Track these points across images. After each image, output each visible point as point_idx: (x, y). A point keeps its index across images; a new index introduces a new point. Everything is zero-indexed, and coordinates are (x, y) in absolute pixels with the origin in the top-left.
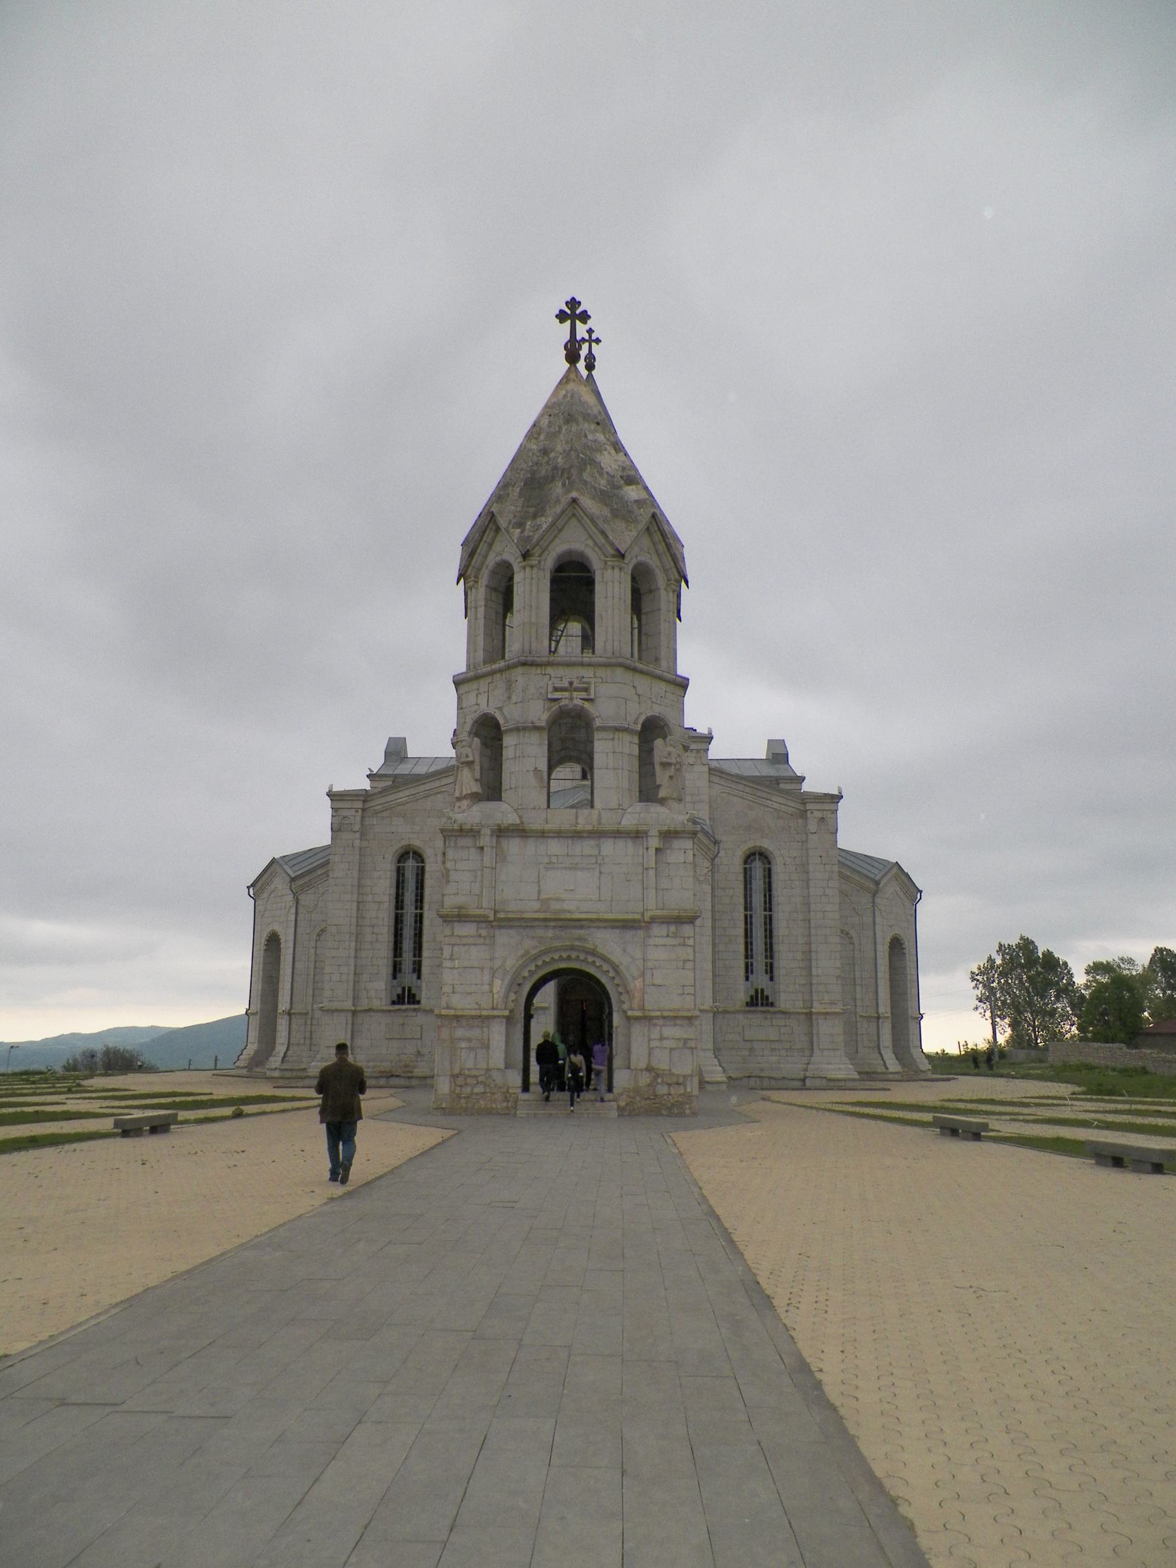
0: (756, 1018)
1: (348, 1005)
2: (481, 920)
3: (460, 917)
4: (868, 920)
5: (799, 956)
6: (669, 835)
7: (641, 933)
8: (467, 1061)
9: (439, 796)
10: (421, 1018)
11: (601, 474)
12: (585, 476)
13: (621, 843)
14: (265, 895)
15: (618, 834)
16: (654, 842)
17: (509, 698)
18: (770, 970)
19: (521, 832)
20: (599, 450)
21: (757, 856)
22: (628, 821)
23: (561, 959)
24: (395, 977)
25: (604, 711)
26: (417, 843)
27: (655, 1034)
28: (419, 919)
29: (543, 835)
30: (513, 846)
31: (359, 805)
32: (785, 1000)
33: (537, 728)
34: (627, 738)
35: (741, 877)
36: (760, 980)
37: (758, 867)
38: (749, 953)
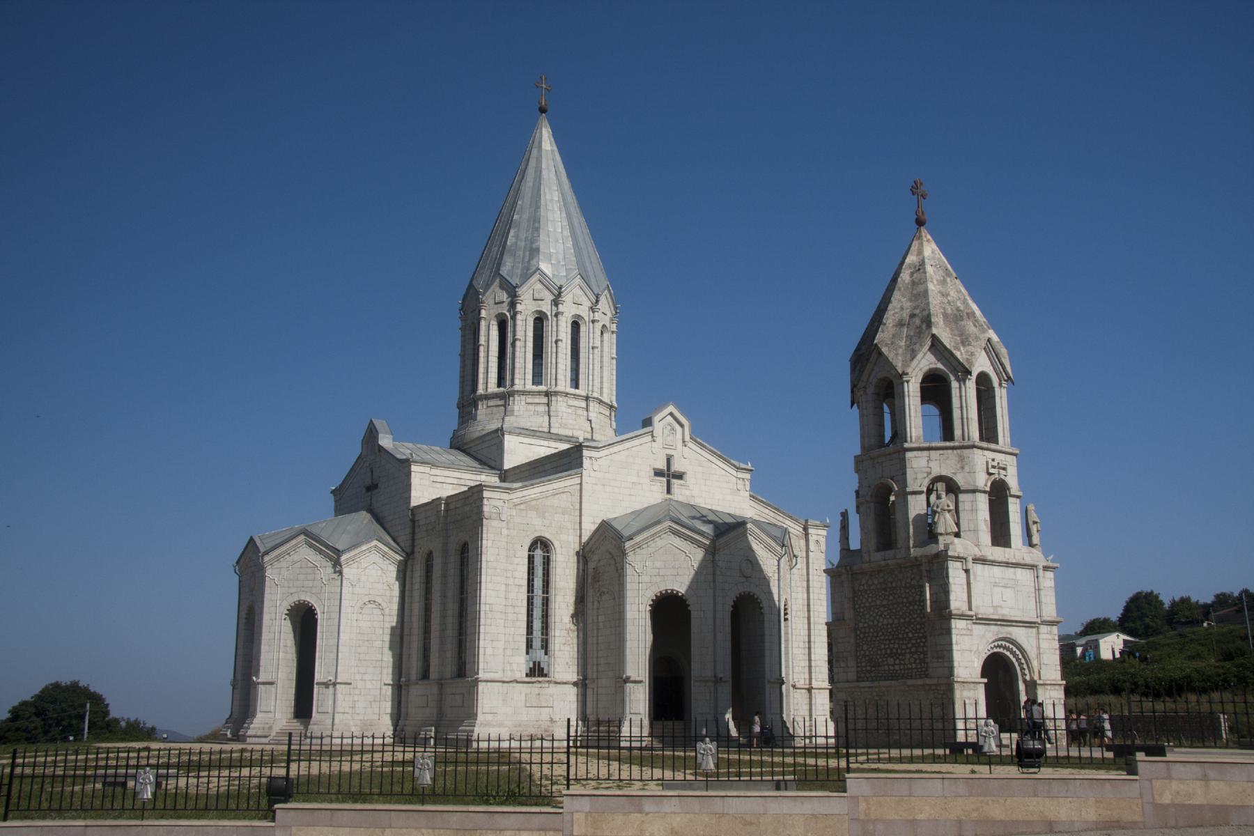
1: (498, 676)
3: (962, 616)
7: (1034, 630)
9: (564, 496)
10: (553, 689)
14: (283, 564)
16: (1041, 572)
17: (963, 468)
22: (1028, 560)
23: (999, 646)
24: (527, 653)
26: (547, 535)
28: (546, 602)
29: (993, 563)
31: (505, 496)
33: (984, 492)
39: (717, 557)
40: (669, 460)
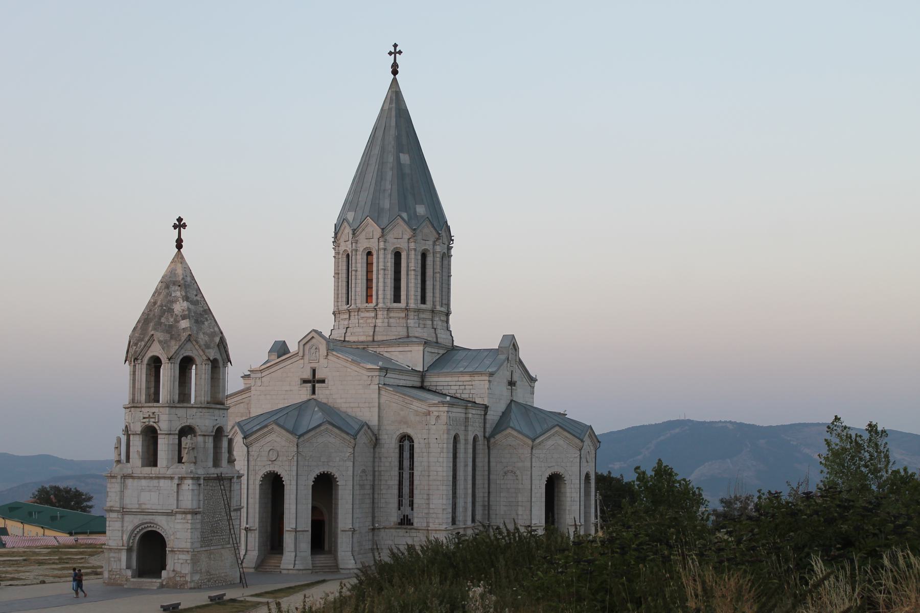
0: (401, 532)
2: (118, 511)
4: (528, 464)
5: (425, 497)
6: (182, 479)
8: (114, 566)
11: (172, 316)
12: (163, 320)
13: (166, 481)
15: (164, 478)
16: (176, 481)
18: (412, 504)
19: (133, 477)
20: (175, 301)
21: (406, 440)
22: (169, 473)
25: (163, 426)
27: (176, 557)
29: (139, 478)
30: (129, 482)
32: (417, 523)
34: (171, 437)
35: (397, 450)
36: (406, 510)
37: (407, 443)
38: (400, 495)
39: (250, 449)
40: (314, 371)
